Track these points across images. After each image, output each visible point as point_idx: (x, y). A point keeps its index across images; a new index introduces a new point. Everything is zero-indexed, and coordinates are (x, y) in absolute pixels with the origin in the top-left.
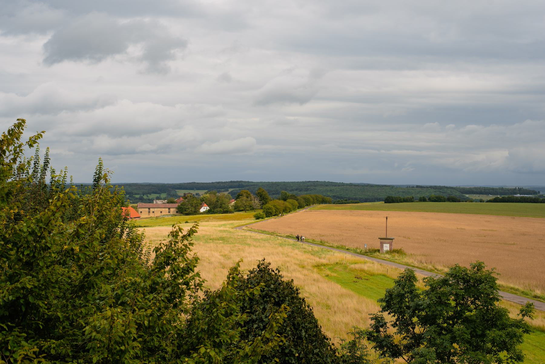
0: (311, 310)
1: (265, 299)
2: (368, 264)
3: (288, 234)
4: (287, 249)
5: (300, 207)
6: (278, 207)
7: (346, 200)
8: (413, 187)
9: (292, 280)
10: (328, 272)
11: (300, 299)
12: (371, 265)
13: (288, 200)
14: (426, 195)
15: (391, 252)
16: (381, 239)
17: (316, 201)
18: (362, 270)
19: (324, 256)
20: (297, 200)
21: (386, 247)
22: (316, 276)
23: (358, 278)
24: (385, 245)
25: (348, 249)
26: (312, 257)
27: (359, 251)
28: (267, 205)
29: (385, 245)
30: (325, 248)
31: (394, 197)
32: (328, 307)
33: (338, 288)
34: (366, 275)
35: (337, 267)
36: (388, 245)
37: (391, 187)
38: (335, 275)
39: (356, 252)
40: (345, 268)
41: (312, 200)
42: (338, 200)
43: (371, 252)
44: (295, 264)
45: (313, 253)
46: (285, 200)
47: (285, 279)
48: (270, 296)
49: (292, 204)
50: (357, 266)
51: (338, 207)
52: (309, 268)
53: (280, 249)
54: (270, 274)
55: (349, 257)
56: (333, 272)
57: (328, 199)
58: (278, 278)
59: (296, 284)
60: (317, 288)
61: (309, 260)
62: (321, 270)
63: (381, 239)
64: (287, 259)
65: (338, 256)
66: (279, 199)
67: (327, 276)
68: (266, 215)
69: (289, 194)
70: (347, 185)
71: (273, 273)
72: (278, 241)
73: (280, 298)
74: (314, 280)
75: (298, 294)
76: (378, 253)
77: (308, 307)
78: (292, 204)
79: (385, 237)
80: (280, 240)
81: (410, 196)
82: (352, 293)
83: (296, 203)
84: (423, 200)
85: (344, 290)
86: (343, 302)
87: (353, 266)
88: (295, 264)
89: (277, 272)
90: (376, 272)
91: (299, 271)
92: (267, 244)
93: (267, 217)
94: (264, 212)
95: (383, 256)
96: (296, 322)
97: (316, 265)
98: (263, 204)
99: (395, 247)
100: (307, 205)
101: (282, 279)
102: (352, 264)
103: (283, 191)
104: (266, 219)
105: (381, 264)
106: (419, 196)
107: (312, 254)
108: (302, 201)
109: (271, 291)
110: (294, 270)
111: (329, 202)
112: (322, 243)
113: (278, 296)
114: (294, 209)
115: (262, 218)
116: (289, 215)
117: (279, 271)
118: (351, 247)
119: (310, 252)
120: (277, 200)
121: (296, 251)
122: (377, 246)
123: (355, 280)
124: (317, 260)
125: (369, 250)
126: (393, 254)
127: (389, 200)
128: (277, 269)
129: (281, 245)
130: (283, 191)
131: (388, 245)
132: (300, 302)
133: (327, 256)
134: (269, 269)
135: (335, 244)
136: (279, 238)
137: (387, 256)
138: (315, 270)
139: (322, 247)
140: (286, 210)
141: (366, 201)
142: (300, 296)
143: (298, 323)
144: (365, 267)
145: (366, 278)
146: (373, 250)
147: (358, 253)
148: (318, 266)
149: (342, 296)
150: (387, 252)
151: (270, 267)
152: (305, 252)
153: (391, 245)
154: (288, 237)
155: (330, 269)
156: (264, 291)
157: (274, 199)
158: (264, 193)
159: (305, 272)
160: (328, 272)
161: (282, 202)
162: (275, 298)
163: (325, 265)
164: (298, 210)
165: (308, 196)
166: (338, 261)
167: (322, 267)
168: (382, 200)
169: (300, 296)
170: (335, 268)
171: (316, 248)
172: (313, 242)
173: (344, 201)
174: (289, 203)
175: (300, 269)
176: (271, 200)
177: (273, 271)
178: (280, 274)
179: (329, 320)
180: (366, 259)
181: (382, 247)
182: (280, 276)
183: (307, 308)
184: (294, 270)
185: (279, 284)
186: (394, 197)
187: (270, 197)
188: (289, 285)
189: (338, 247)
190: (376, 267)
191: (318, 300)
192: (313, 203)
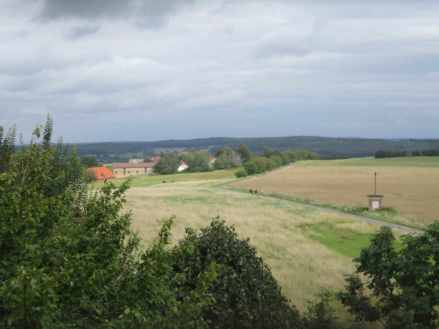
0: (269, 270)
1: (218, 259)
2: (356, 224)
3: (271, 193)
4: (270, 209)
5: (285, 163)
6: (261, 164)
7: (334, 156)
8: (406, 141)
9: (248, 239)
10: (313, 232)
11: (257, 258)
12: (359, 224)
13: (272, 157)
14: (420, 148)
15: (381, 210)
16: (370, 196)
17: (301, 157)
18: (349, 230)
19: (308, 215)
20: (281, 156)
21: (376, 205)
22: (299, 236)
23: (344, 238)
24: (373, 203)
25: (334, 208)
26: (296, 216)
27: (346, 209)
28: (249, 162)
29: (373, 203)
30: (310, 207)
31: (384, 151)
32: (311, 269)
33: (323, 249)
34: (353, 235)
35: (322, 227)
36: (377, 203)
37: (383, 141)
38: (320, 235)
39: (342, 210)
40: (331, 227)
41: (296, 156)
42: (325, 155)
43: (360, 211)
44: (277, 224)
45: (297, 212)
46: (268, 156)
47: (240, 238)
48: (224, 256)
49: (276, 161)
50: (343, 226)
51: (325, 163)
52: (292, 228)
53: (262, 208)
54: (224, 233)
55: (335, 215)
56: (318, 232)
57: (312, 154)
58: (232, 237)
59: (252, 243)
60: (300, 249)
61: (292, 220)
62: (305, 230)
63: (370, 196)
64: (269, 219)
65: (322, 215)
66: (262, 156)
67: (311, 236)
68: (248, 172)
69: (272, 150)
70: (335, 139)
71: (228, 232)
72: (260, 200)
73: (234, 257)
74: (297, 241)
75: (254, 253)
76: (366, 212)
77: (266, 267)
78: (276, 161)
79: (374, 194)
80: (262, 199)
81: (402, 150)
82: (337, 254)
83: (280, 159)
84: (416, 154)
85: (329, 251)
86: (328, 263)
87: (339, 225)
88: (277, 224)
89: (231, 230)
90: (364, 232)
91: (281, 232)
92: (248, 204)
93: (249, 175)
94: (246, 169)
95: (371, 214)
96: (251, 283)
97: (299, 224)
98: (245, 161)
99: (385, 204)
100: (292, 162)
101: (237, 238)
102: (338, 223)
103: (266, 147)
104: (248, 177)
105: (369, 223)
106: (412, 150)
107: (296, 214)
108: (287, 158)
109: (225, 250)
110: (276, 231)
111: (315, 158)
112: (307, 202)
113: (232, 256)
114: (278, 166)
115: (244, 176)
116: (273, 172)
117: (234, 230)
118: (339, 205)
119: (293, 211)
120: (260, 157)
121: (279, 210)
122: (366, 204)
123: (341, 240)
124: (301, 219)
125: (357, 208)
126: (382, 212)
127: (380, 155)
128: (231, 227)
129: (263, 204)
130: (266, 147)
131: (377, 203)
132: (257, 262)
133: (312, 215)
134: (224, 228)
135: (321, 203)
136: (261, 197)
137: (377, 214)
138: (299, 230)
139: (307, 206)
140: (269, 168)
141: (355, 156)
142: (257, 255)
143: (253, 284)
144: (352, 227)
145: (353, 238)
146: (361, 208)
147: (345, 212)
148: (302, 227)
149: (326, 257)
150: (376, 210)
151: (225, 225)
152: (288, 211)
153: (380, 202)
154: (271, 195)
155: (314, 229)
156: (217, 250)
157: (256, 156)
158: (246, 150)
159: (288, 232)
160: (313, 232)
161: (265, 158)
162: (228, 258)
163: (309, 225)
164: (282, 167)
165: (292, 152)
166: (323, 220)
167: (306, 227)
168: (373, 156)
169: (257, 255)
170: (320, 228)
171: (300, 207)
172: (298, 201)
173: (332, 157)
174: (273, 159)
175: (283, 230)
176: (253, 157)
177: (228, 229)
178: (235, 232)
179: (311, 282)
180: (354, 218)
181: (371, 204)
182: (234, 234)
183: (264, 268)
184: (276, 231)
185: (234, 243)
186: (384, 151)
187: (252, 154)
188: (244, 243)
189: (324, 206)
190: (363, 226)
191: (301, 261)
192: (299, 159)
